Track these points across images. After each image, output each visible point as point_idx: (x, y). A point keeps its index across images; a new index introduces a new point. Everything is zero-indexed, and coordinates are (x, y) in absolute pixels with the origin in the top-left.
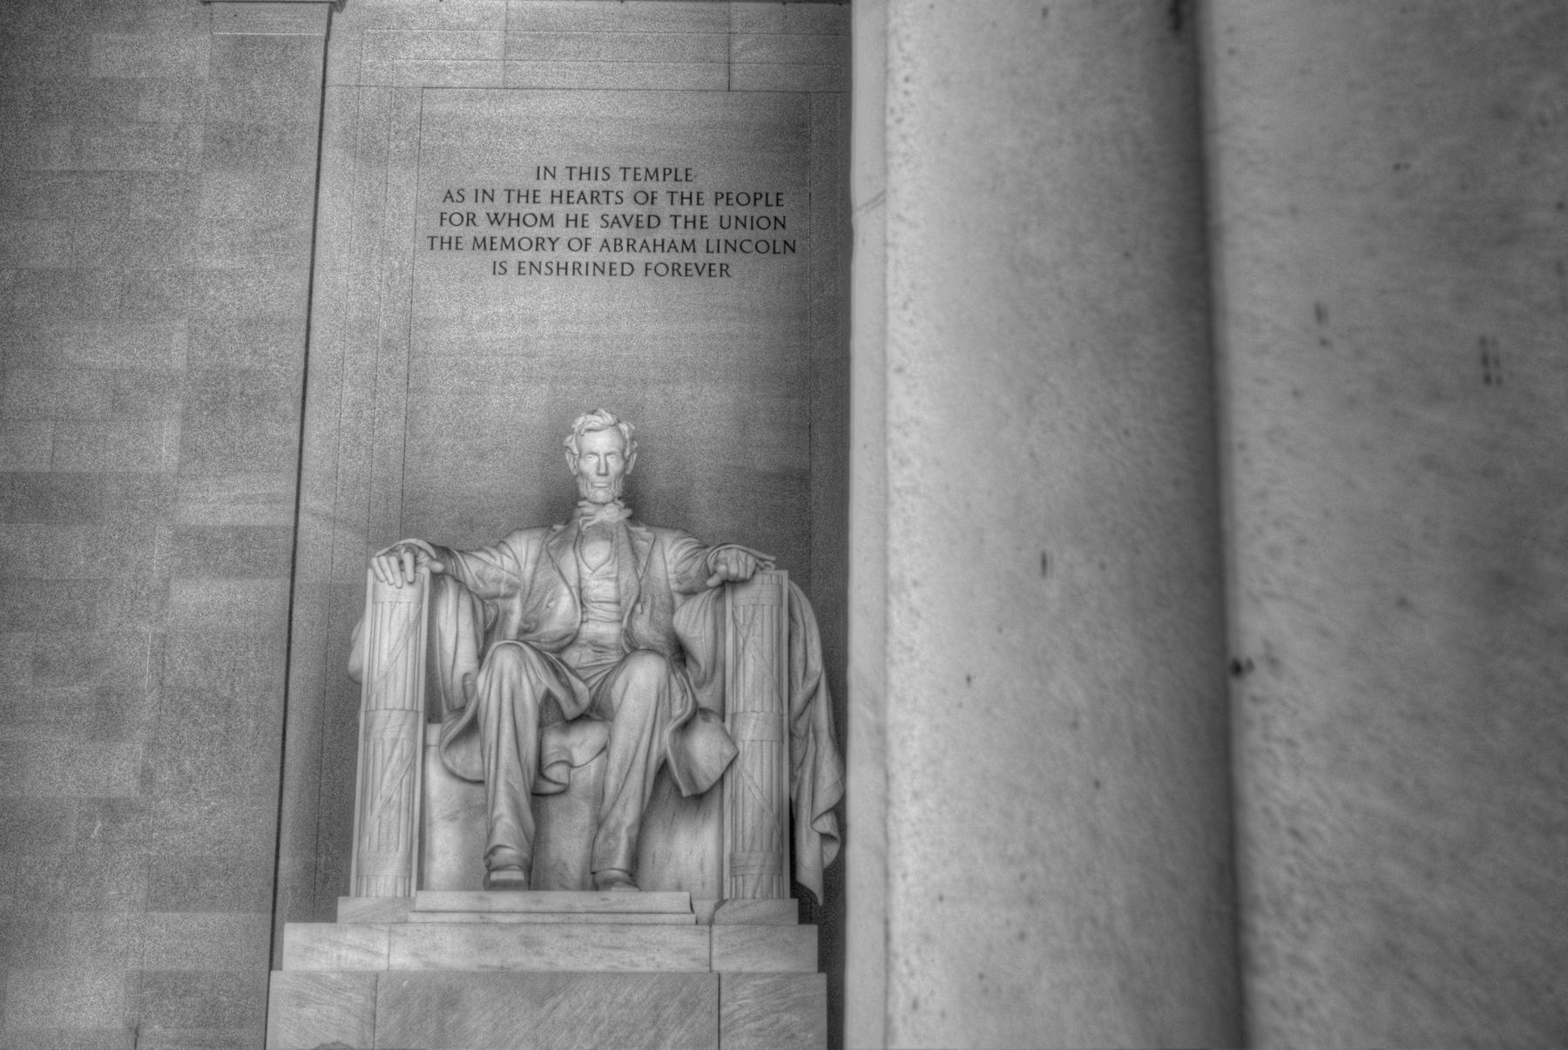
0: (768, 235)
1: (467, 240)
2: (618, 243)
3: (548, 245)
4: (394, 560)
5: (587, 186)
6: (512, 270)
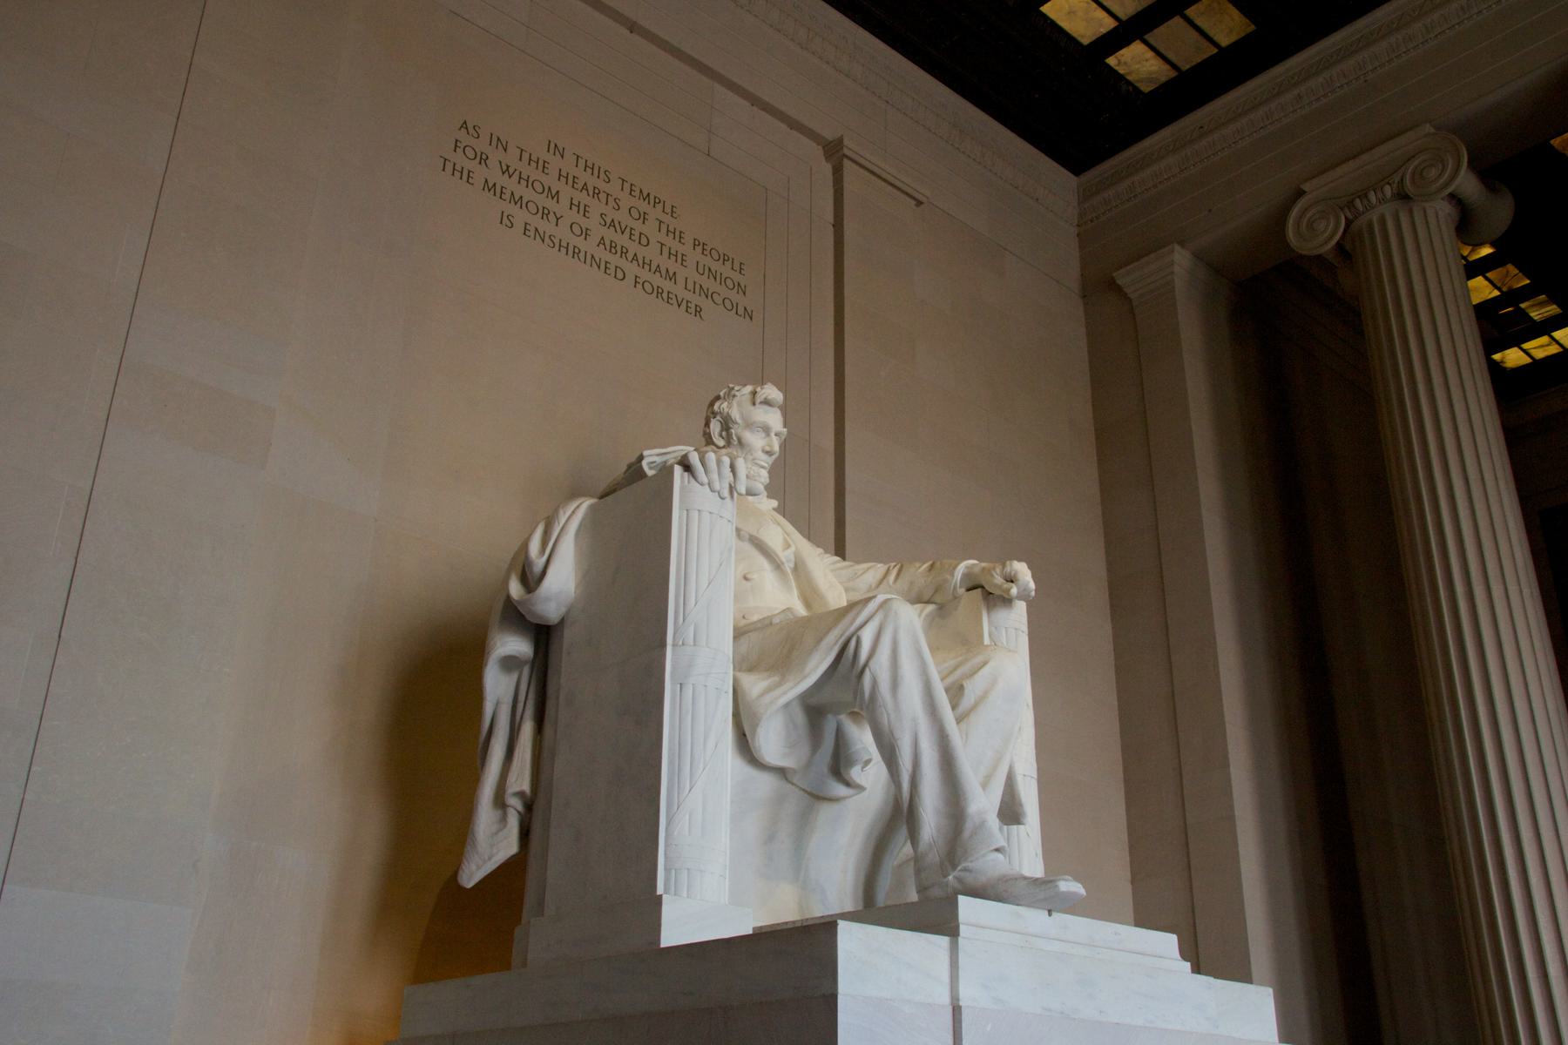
0: (735, 296)
1: (478, 180)
2: (613, 246)
3: (551, 216)
4: (726, 460)
5: (592, 182)
6: (519, 227)
